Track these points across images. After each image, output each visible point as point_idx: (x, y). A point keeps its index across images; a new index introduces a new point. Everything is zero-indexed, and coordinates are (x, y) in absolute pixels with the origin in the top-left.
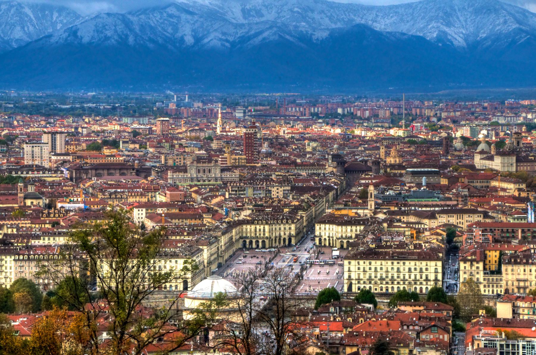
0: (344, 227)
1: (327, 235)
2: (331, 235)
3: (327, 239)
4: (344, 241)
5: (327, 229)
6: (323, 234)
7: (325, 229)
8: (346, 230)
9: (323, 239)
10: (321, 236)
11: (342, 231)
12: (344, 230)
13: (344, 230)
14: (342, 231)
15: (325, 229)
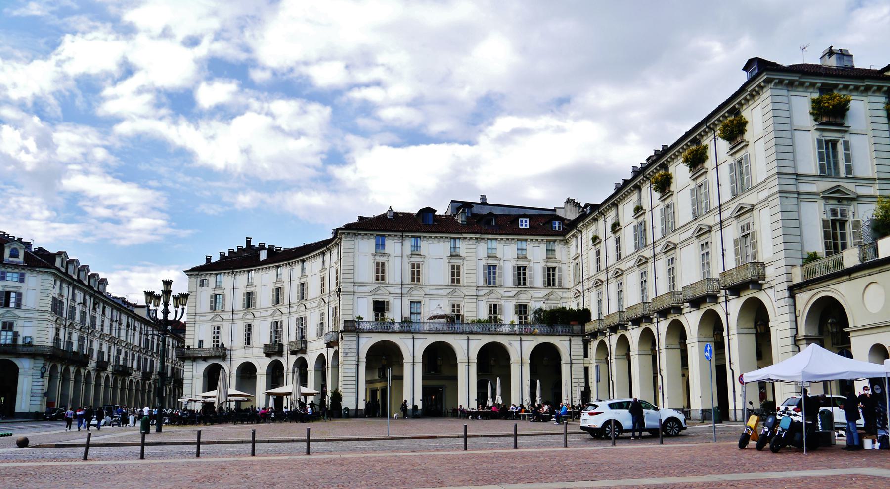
0: (394, 246)
1: (262, 336)
2: (289, 336)
3: (262, 365)
4: (404, 343)
5: (264, 298)
6: (233, 337)
7: (249, 300)
8: (416, 273)
9: (230, 368)
10: (221, 352)
11: (380, 273)
12: (396, 271)
13: (396, 271)
14: (380, 273)
15: (249, 300)
